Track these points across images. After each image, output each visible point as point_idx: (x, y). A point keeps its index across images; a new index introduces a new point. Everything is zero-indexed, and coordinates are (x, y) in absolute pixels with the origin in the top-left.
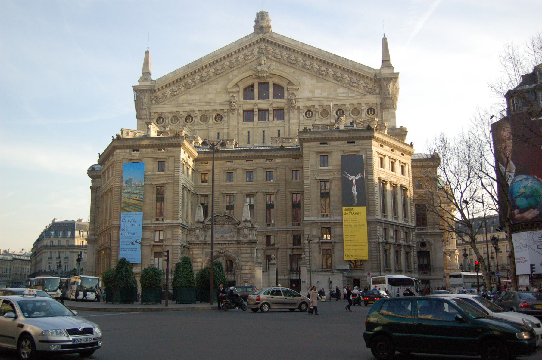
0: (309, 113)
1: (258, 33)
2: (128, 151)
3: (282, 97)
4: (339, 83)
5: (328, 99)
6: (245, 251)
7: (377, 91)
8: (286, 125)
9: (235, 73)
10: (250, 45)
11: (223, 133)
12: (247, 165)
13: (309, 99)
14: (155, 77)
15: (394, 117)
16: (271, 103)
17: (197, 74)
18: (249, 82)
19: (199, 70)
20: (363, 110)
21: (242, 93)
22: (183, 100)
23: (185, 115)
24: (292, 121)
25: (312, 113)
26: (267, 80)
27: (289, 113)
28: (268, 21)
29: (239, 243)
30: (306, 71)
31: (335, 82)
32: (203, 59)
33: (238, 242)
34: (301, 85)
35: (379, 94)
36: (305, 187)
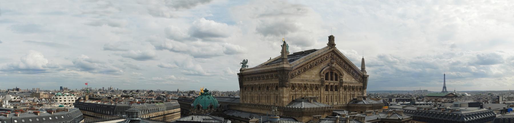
0: (345, 88)
5: (351, 83)
9: (322, 65)
18: (328, 71)
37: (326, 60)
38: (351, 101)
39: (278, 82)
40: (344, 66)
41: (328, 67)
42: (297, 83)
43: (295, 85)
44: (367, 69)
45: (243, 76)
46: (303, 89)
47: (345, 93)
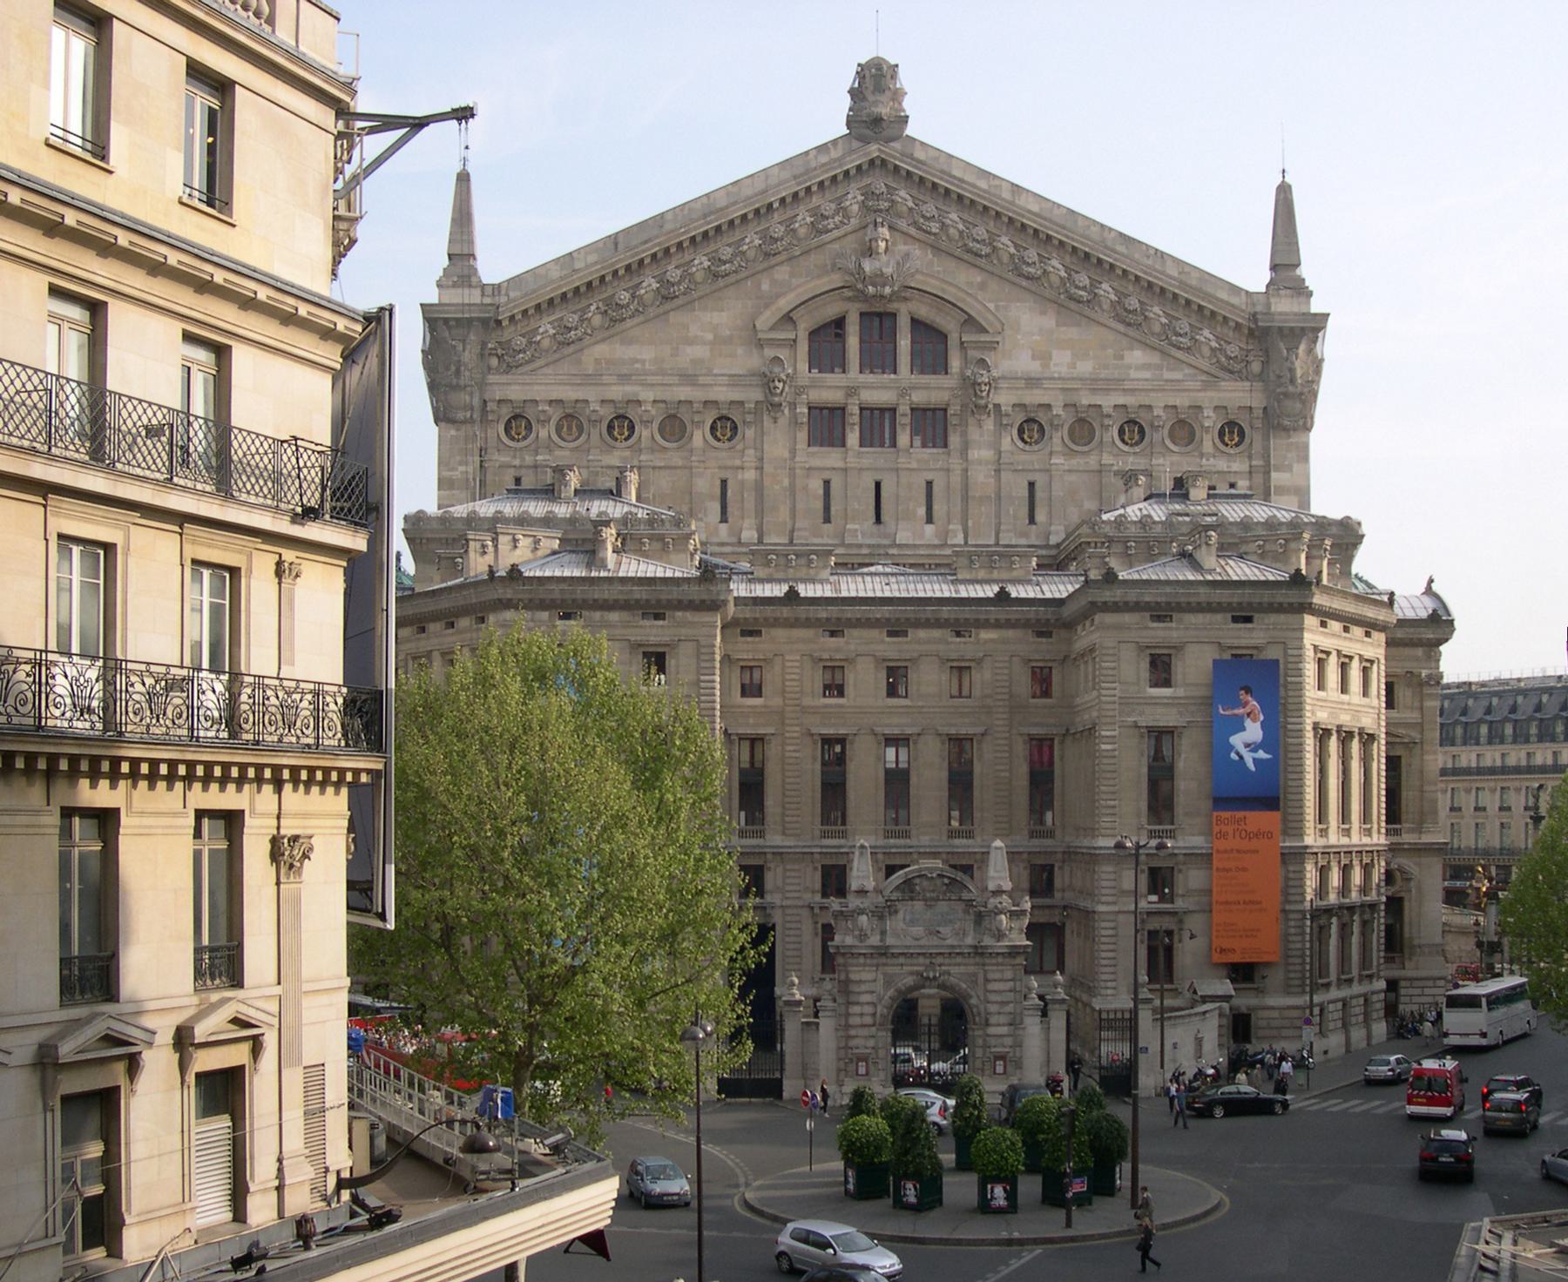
0: (1031, 427)
1: (866, 141)
2: (545, 615)
5: (1095, 384)
6: (998, 976)
7: (1256, 367)
8: (956, 463)
9: (782, 273)
10: (834, 178)
11: (742, 483)
12: (891, 648)
13: (1032, 382)
14: (494, 267)
15: (1305, 458)
16: (902, 386)
17: (648, 272)
18: (831, 311)
19: (654, 256)
20: (1207, 429)
21: (803, 347)
23: (607, 413)
24: (974, 454)
25: (1042, 430)
26: (892, 307)
27: (964, 423)
28: (898, 95)
29: (982, 954)
30: (1024, 283)
31: (1121, 327)
32: (669, 217)
33: (978, 951)
34: (1008, 332)
35: (1261, 377)
36: (1104, 747)
43: (530, 413)
46: (595, 433)
47: (1031, 458)
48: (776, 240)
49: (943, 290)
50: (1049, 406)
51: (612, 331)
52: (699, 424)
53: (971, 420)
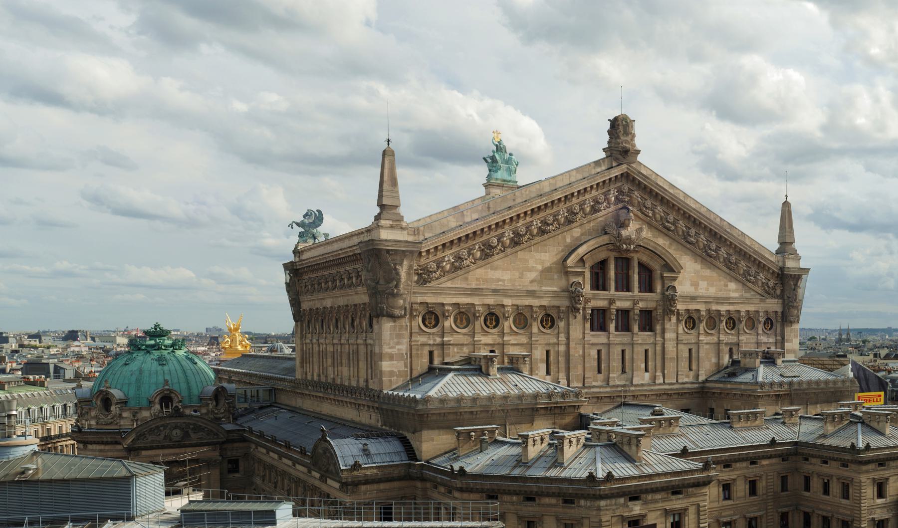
0: (692, 321)
3: (651, 289)
4: (732, 273)
5: (719, 301)
7: (778, 292)
9: (577, 232)
13: (693, 299)
16: (635, 299)
18: (602, 256)
19: (511, 218)
21: (588, 275)
22: (478, 280)
24: (668, 335)
31: (727, 271)
37: (594, 210)
38: (719, 369)
39: (365, 299)
40: (686, 236)
41: (605, 239)
42: (447, 300)
44: (800, 243)
45: (302, 276)
48: (576, 214)
49: (655, 248)
50: (698, 311)
51: (486, 261)
52: (535, 319)
53: (666, 318)
